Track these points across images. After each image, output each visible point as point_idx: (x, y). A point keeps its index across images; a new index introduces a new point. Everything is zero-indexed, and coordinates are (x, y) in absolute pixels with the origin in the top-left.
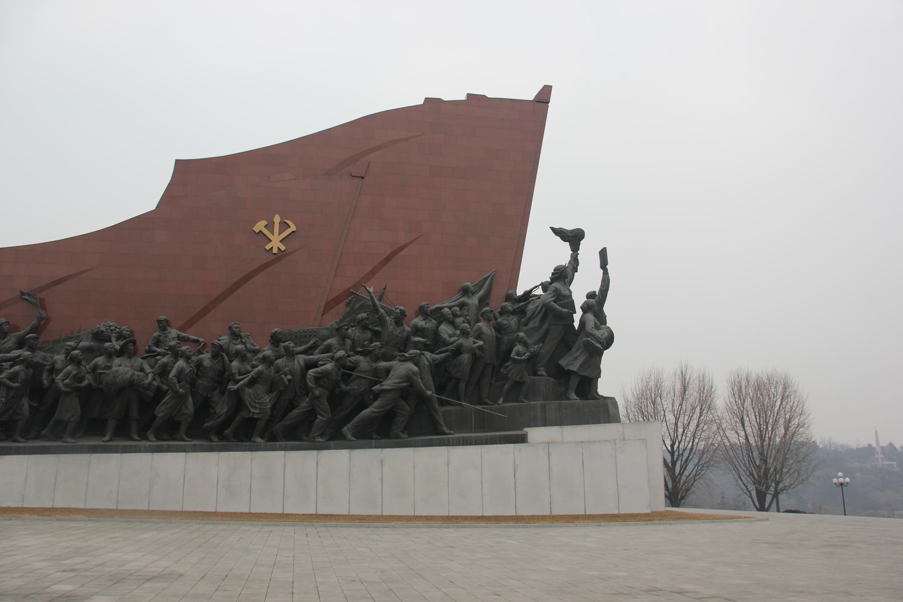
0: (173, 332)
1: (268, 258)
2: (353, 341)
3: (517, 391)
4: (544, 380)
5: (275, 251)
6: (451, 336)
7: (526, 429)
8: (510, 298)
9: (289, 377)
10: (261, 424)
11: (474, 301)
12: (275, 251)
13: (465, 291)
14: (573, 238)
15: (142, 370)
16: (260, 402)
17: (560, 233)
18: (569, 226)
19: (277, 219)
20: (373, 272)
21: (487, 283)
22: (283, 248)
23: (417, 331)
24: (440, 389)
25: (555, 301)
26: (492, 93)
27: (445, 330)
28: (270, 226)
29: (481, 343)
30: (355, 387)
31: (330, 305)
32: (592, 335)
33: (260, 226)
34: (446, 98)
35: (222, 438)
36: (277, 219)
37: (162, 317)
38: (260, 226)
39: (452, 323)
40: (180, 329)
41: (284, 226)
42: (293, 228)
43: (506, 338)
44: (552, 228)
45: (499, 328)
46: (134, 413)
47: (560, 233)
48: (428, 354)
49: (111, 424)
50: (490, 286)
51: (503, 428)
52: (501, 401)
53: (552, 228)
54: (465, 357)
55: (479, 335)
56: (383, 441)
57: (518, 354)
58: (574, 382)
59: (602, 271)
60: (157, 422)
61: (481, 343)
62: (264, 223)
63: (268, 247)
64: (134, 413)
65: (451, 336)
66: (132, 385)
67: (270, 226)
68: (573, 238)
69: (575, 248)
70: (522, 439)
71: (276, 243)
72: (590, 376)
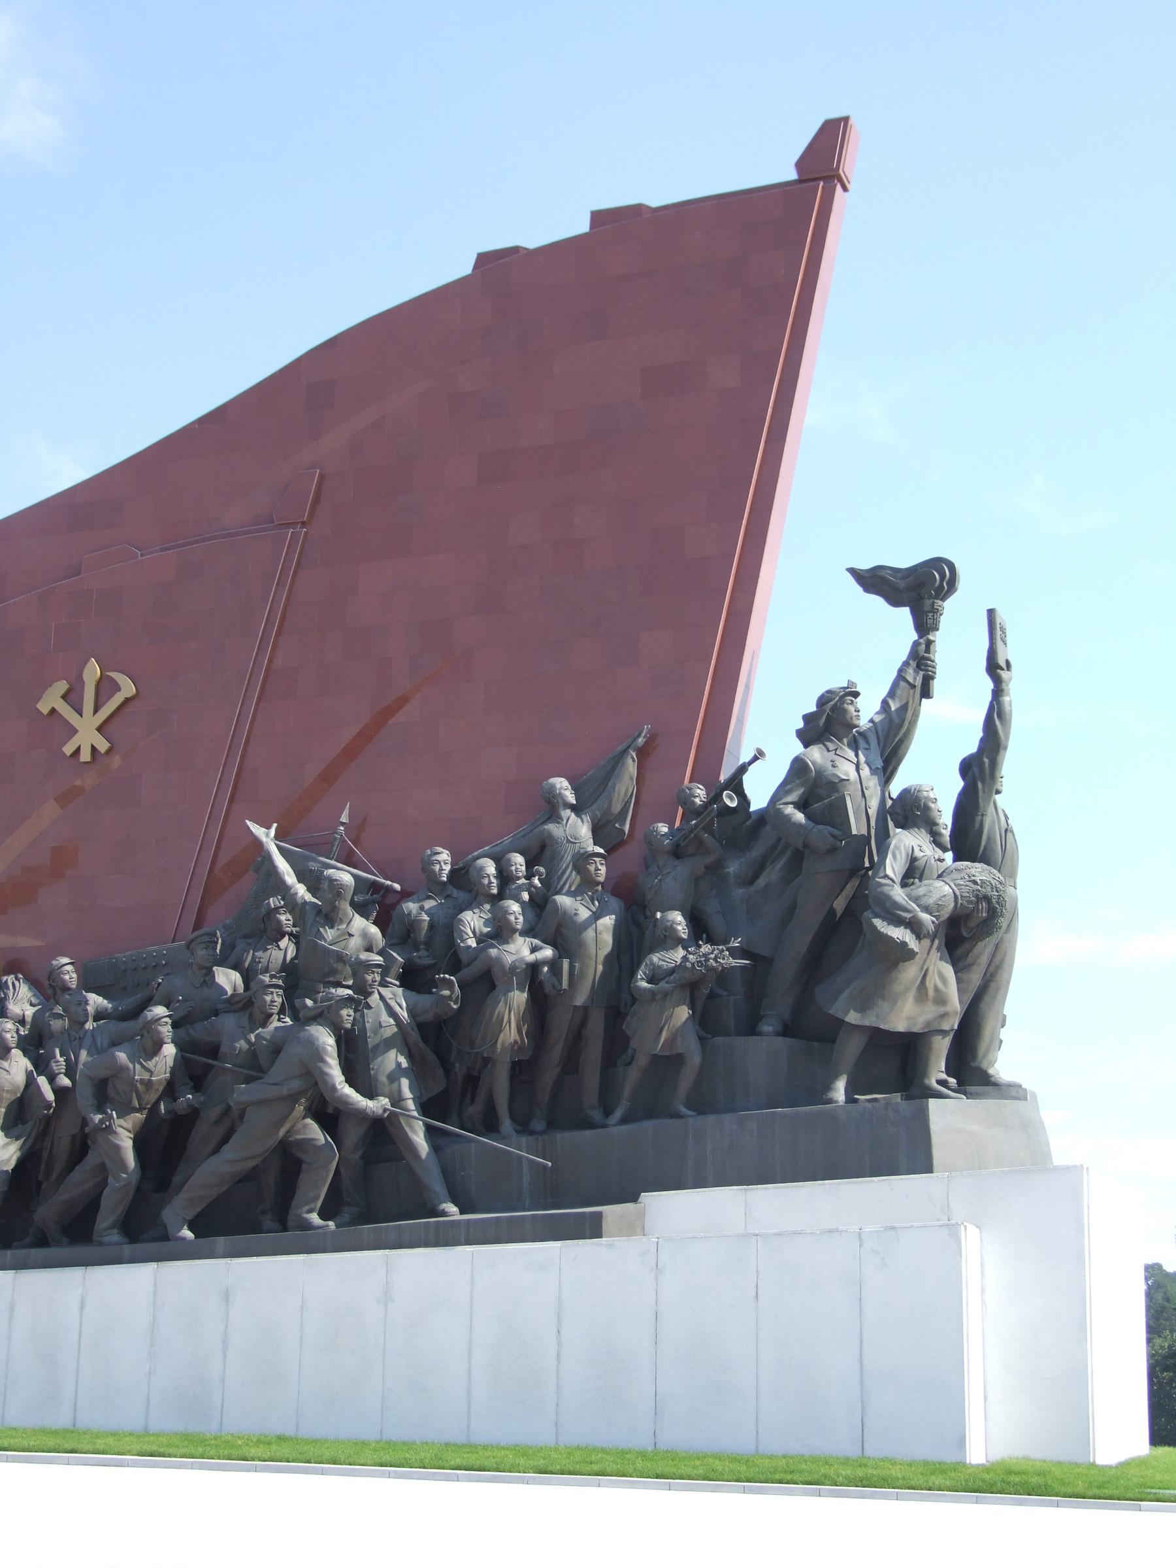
5: (85, 756)
9: (65, 1081)
14: (918, 589)
17: (875, 581)
18: (904, 556)
19: (93, 671)
22: (103, 746)
28: (72, 697)
33: (52, 700)
34: (533, 240)
36: (93, 671)
38: (52, 700)
41: (105, 688)
42: (128, 688)
44: (853, 571)
47: (875, 581)
51: (568, 1204)
53: (853, 571)
56: (221, 1242)
58: (851, 1049)
59: (989, 685)
61: (548, 952)
62: (62, 686)
63: (68, 749)
67: (72, 697)
68: (918, 589)
69: (925, 624)
71: (87, 735)
72: (917, 1029)
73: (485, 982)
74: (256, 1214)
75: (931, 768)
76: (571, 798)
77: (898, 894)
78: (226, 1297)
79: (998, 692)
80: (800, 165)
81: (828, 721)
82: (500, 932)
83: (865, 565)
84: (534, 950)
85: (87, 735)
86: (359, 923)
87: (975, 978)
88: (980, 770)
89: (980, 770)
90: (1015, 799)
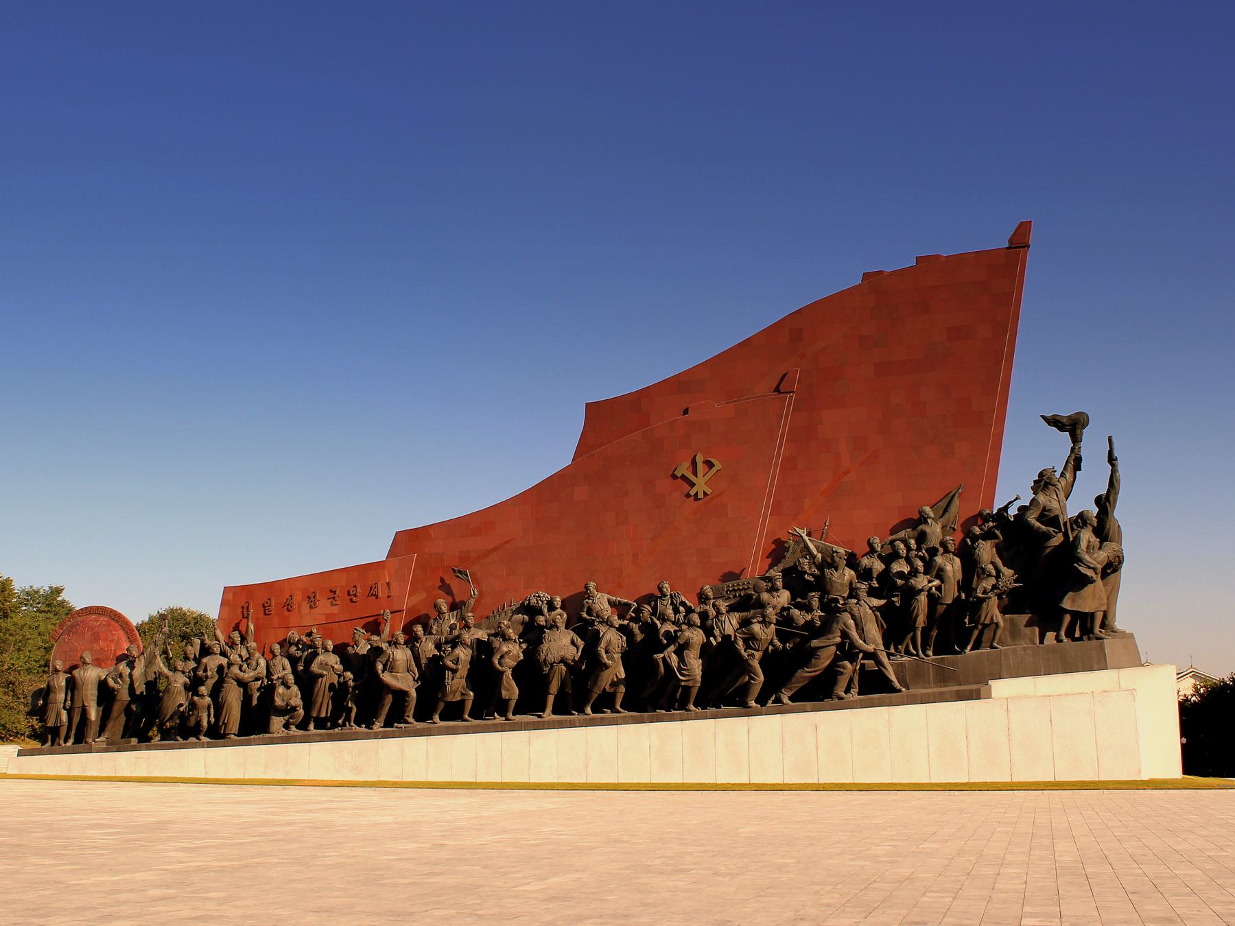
7: (991, 682)
10: (694, 692)
12: (701, 495)
17: (1055, 422)
18: (1065, 412)
19: (700, 459)
22: (709, 491)
25: (1038, 519)
26: (947, 250)
29: (937, 582)
33: (684, 469)
39: (908, 561)
47: (1055, 422)
55: (940, 574)
61: (937, 582)
63: (692, 493)
68: (1073, 426)
69: (1076, 439)
75: (1080, 502)
76: (932, 515)
79: (1114, 471)
80: (1010, 241)
81: (1043, 483)
82: (914, 572)
83: (1048, 414)
84: (930, 582)
86: (847, 570)
87: (1109, 588)
88: (1105, 503)
89: (1105, 503)
90: (1120, 513)
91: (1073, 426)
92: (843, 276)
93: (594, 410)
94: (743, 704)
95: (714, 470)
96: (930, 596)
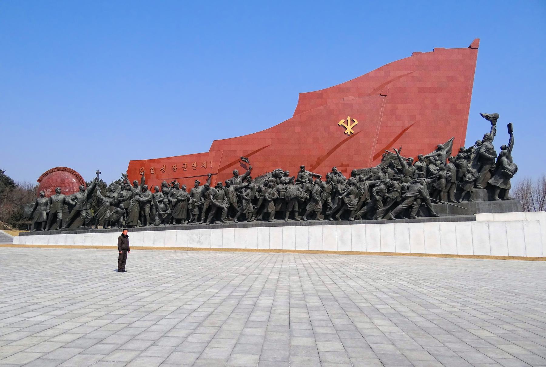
0: (307, 172)
1: (346, 136)
2: (389, 174)
3: (468, 196)
4: (482, 191)
5: (349, 133)
6: (435, 170)
7: (476, 215)
8: (461, 151)
9: (363, 191)
11: (444, 153)
12: (349, 133)
13: (439, 149)
15: (298, 190)
16: (353, 202)
18: (489, 113)
19: (349, 119)
20: (395, 140)
21: (450, 144)
22: (353, 132)
23: (420, 169)
24: (431, 195)
26: (447, 46)
27: (432, 167)
30: (394, 195)
31: (375, 158)
32: (507, 168)
33: (342, 122)
35: (336, 219)
36: (349, 119)
37: (303, 166)
40: (309, 171)
42: (356, 122)
43: (461, 170)
45: (458, 166)
46: (297, 209)
48: (426, 180)
49: (288, 214)
50: (452, 145)
52: (461, 200)
54: (443, 180)
55: (449, 170)
57: (469, 178)
58: (498, 191)
60: (308, 212)
61: (450, 173)
62: (343, 121)
64: (297, 209)
65: (435, 170)
66: (297, 198)
68: (493, 119)
70: (474, 219)
73: (440, 177)
74: (405, 215)
77: (508, 167)
78: (409, 229)
83: (482, 113)
85: (349, 130)
91: (493, 119)
92: (403, 54)
93: (303, 97)
94: (376, 219)
95: (355, 124)
96: (447, 179)
